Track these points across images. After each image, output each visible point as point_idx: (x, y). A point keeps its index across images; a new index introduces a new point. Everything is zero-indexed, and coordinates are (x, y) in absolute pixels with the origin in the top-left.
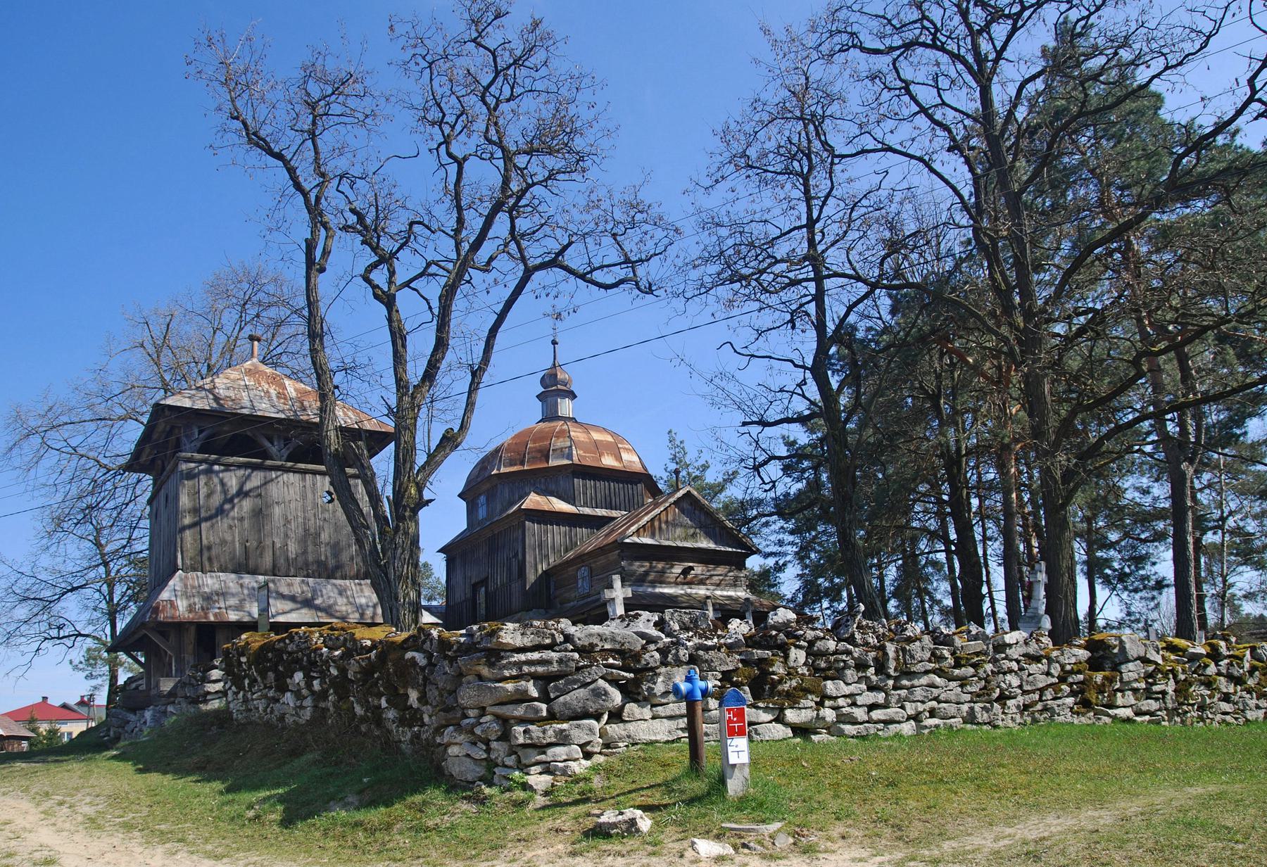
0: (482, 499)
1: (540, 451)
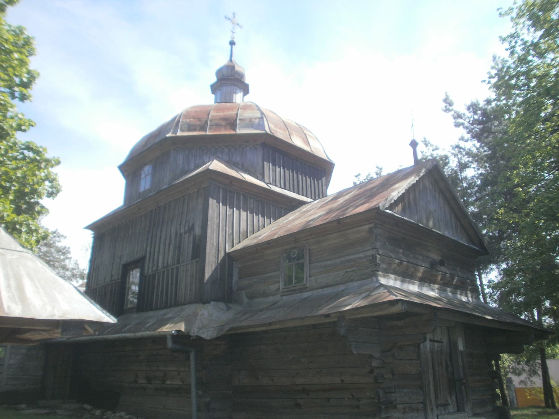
1: (225, 119)
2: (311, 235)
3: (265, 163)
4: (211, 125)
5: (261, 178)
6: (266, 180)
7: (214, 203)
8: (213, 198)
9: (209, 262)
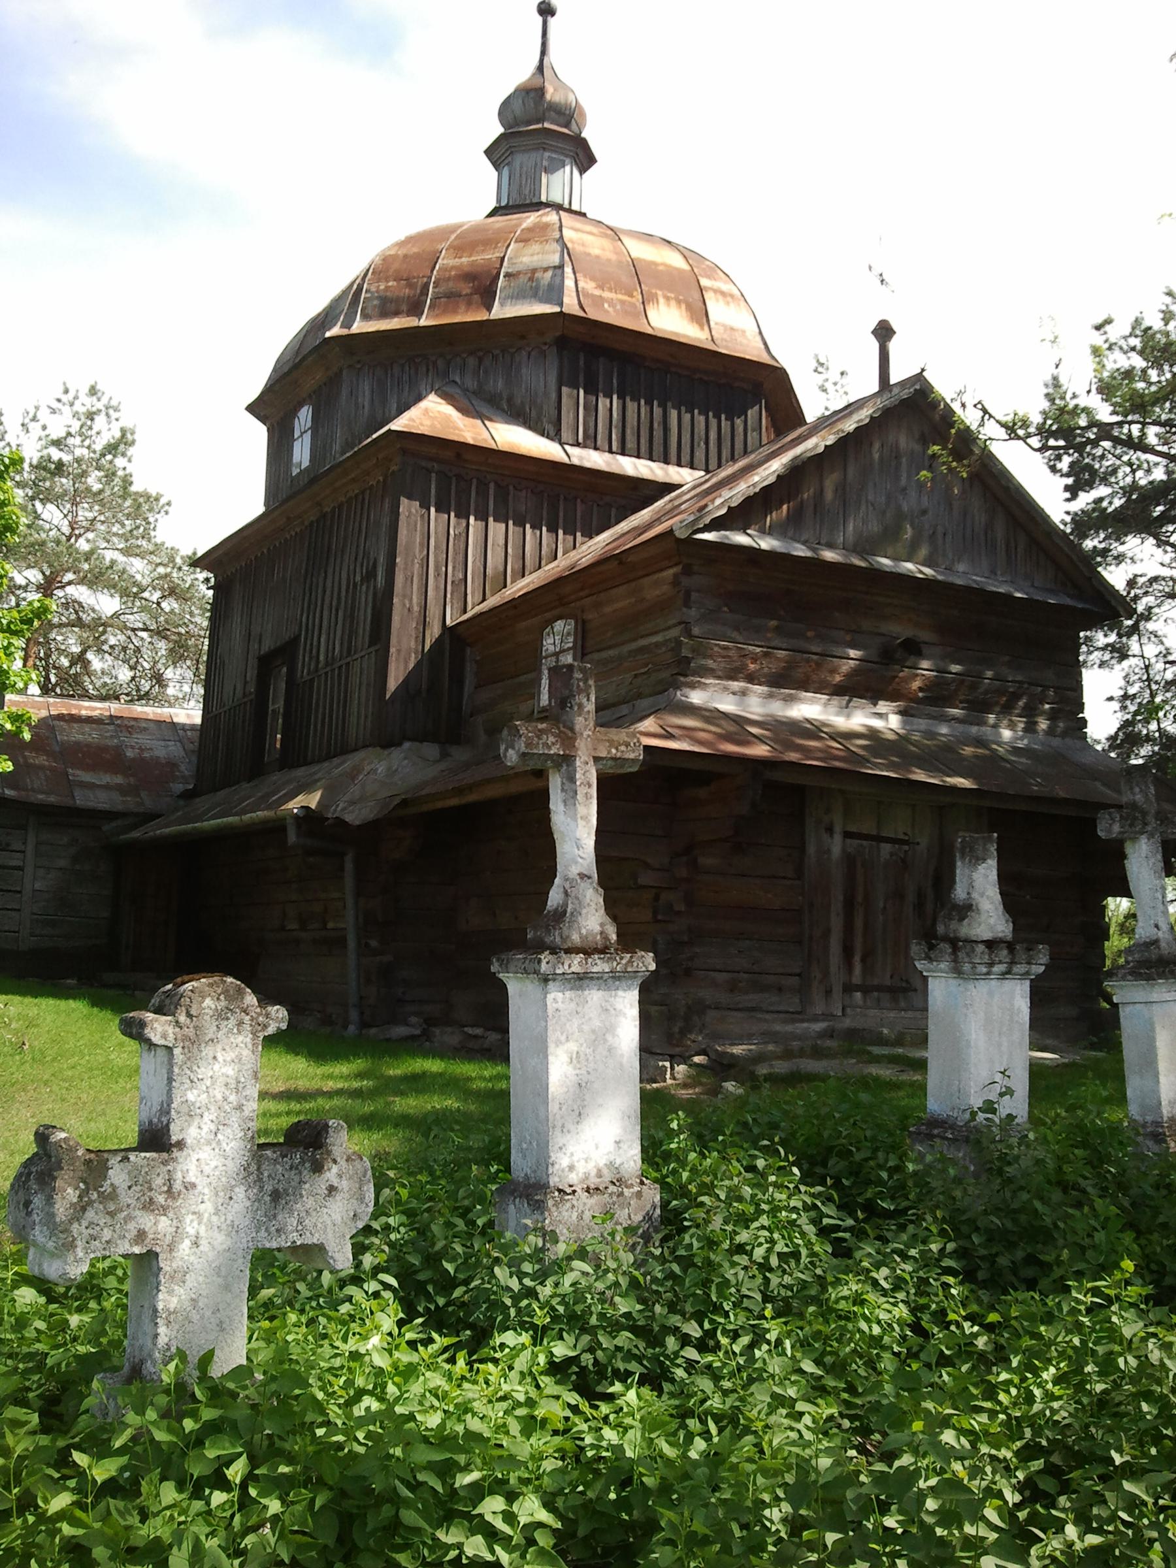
0: (305, 415)
1: (469, 276)
2: (582, 589)
3: (565, 390)
4: (436, 298)
5: (552, 433)
6: (566, 435)
7: (413, 511)
8: (410, 497)
9: (399, 651)
